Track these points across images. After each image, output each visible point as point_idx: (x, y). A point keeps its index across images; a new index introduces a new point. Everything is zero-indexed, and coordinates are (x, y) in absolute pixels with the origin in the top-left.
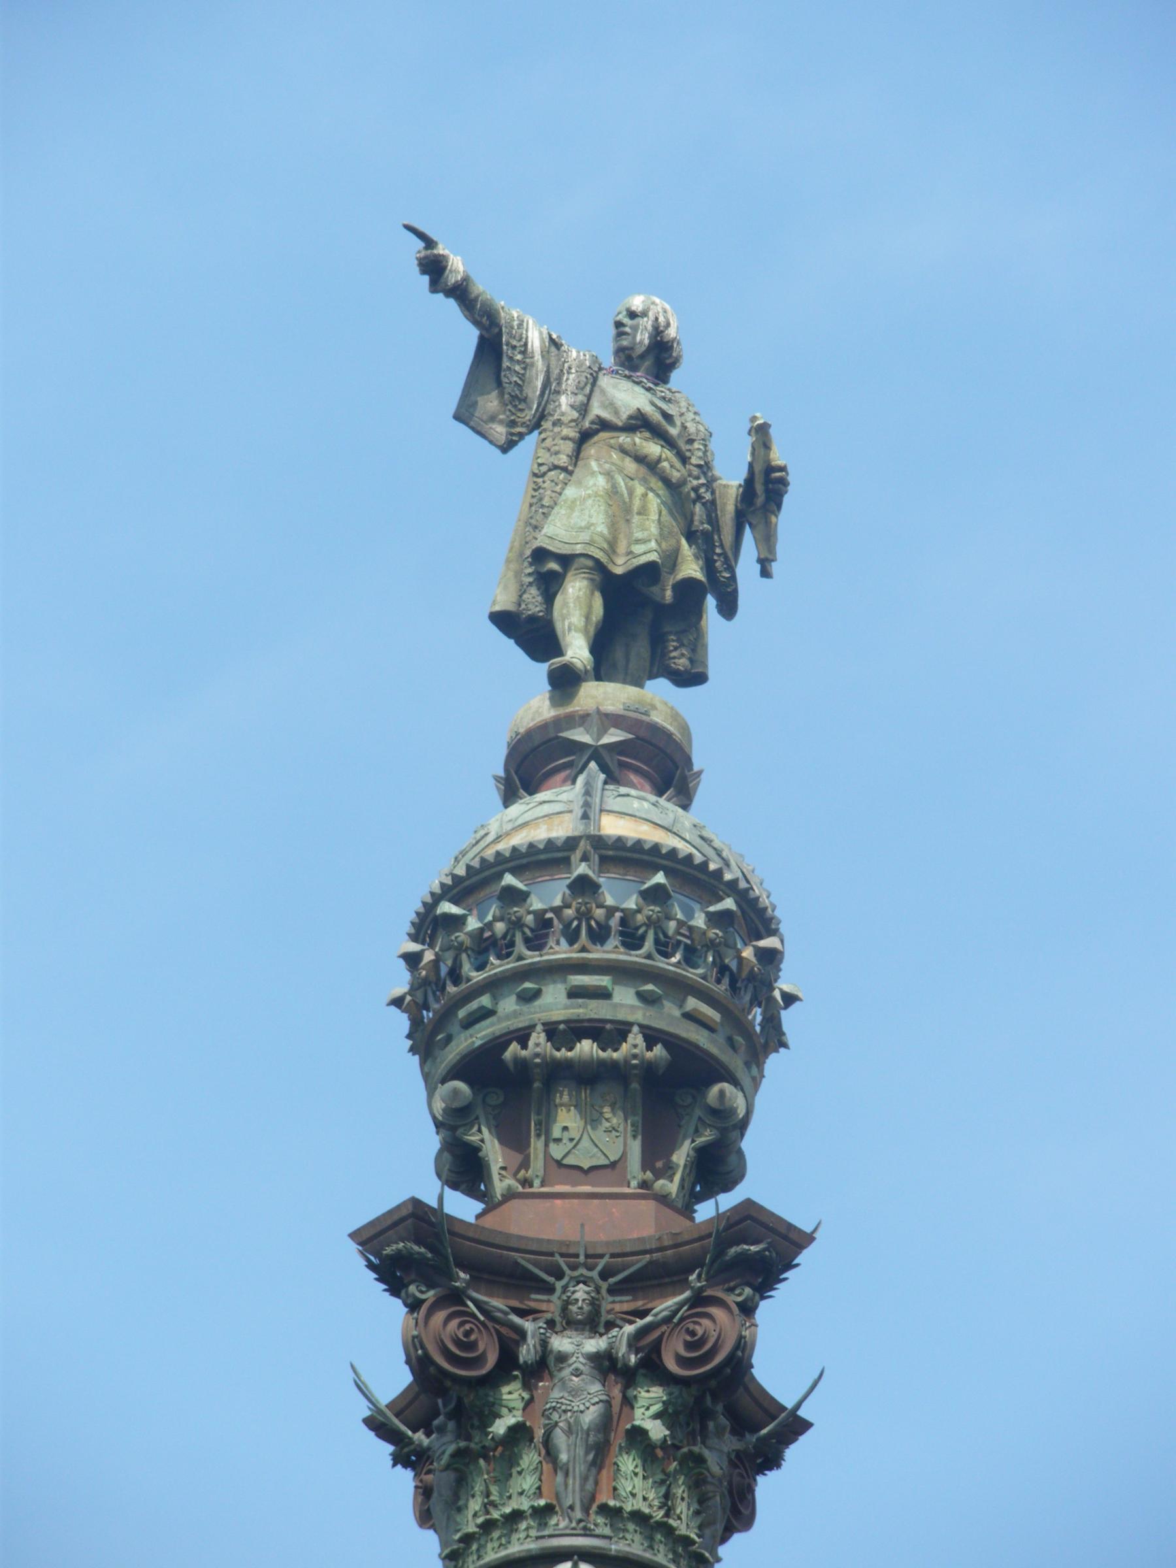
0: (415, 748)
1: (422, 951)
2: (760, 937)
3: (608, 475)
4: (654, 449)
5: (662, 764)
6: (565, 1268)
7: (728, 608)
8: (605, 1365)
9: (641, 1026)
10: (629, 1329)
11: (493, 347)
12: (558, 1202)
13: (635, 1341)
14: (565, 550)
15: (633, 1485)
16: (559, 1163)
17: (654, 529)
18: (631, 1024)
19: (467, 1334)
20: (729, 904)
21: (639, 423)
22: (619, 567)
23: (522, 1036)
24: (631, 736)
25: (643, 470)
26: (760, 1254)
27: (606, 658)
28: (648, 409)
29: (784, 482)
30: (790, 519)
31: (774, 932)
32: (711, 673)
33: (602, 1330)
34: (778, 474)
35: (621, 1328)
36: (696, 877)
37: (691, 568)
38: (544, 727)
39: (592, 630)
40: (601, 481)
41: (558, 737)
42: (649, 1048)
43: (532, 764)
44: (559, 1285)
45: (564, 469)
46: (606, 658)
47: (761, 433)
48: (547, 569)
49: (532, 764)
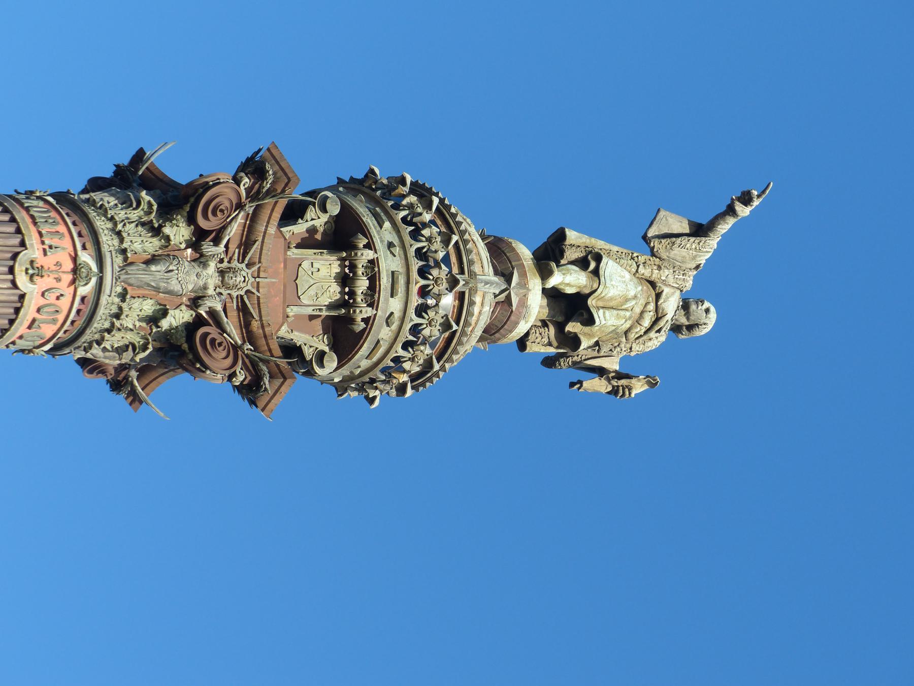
3: (635, 297)
4: (647, 323)
9: (375, 315)
12: (282, 265)
14: (601, 272)
16: (300, 265)
17: (610, 323)
18: (377, 310)
22: (591, 302)
23: (368, 246)
25: (636, 316)
39: (561, 287)
40: (632, 293)
41: (513, 268)
42: (363, 320)
44: (243, 266)
45: (637, 271)
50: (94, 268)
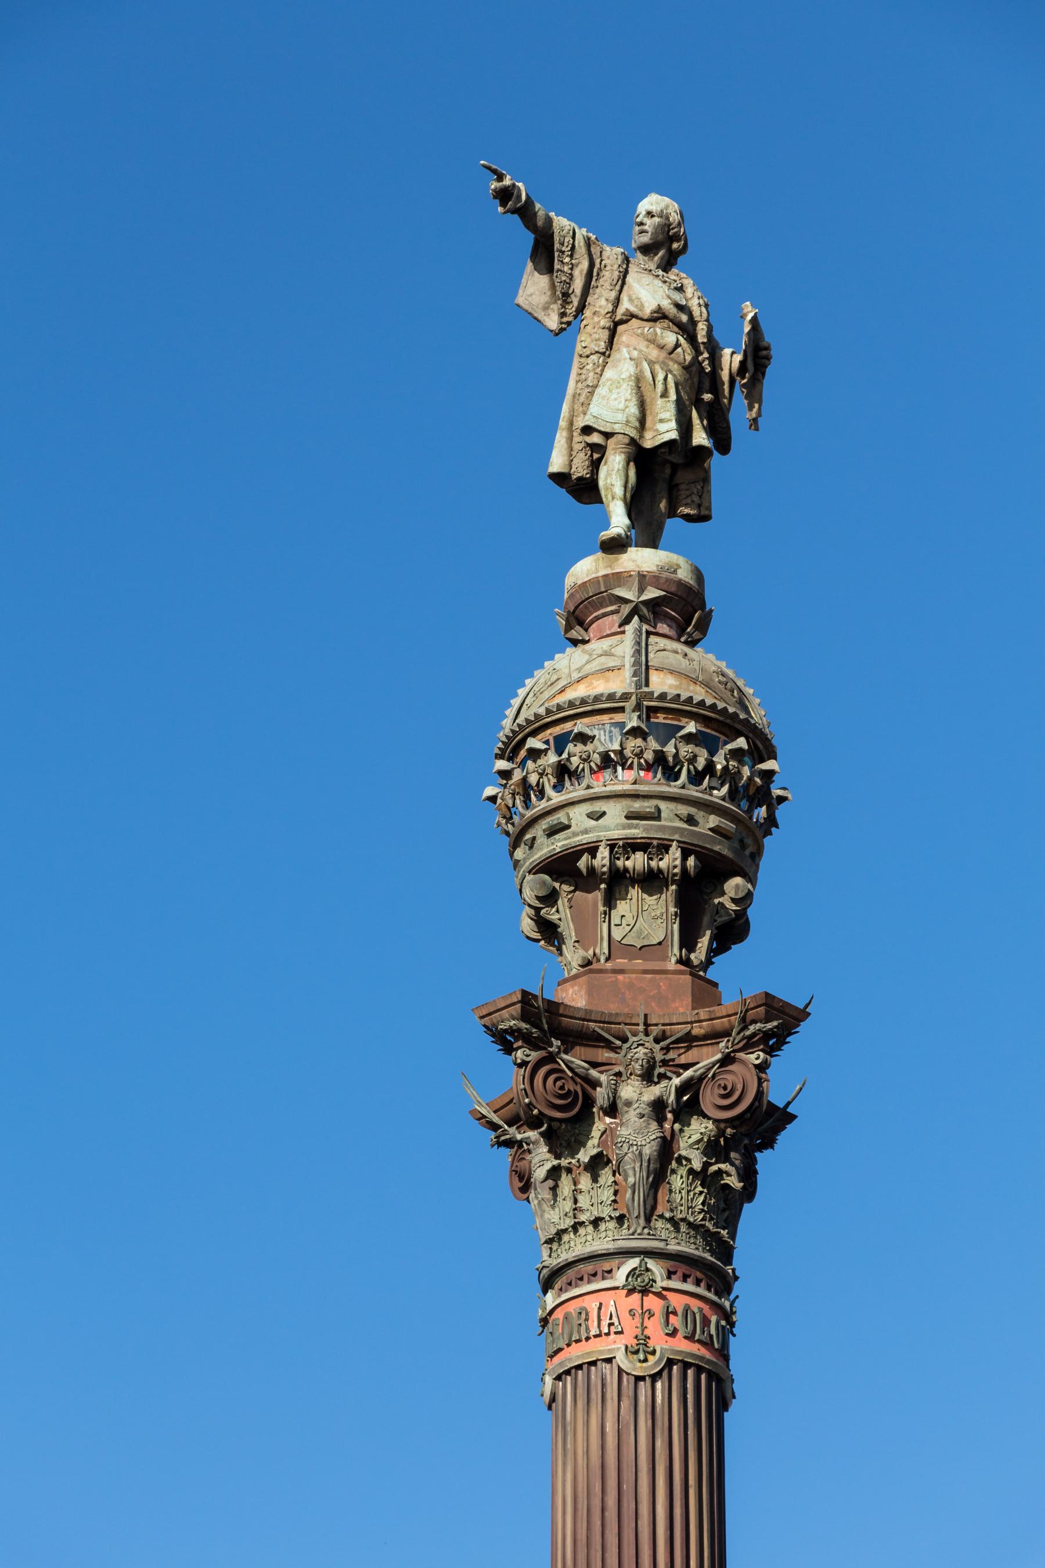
1: (513, 769)
2: (762, 761)
6: (629, 1035)
8: (658, 1107)
9: (678, 841)
10: (677, 1081)
12: (620, 977)
13: (681, 1091)
14: (608, 430)
18: (673, 841)
19: (562, 1088)
20: (741, 742)
24: (663, 593)
28: (666, 304)
29: (768, 358)
31: (773, 756)
32: (714, 513)
33: (656, 1080)
34: (765, 352)
35: (670, 1079)
38: (595, 581)
45: (603, 354)
50: (633, 1263)
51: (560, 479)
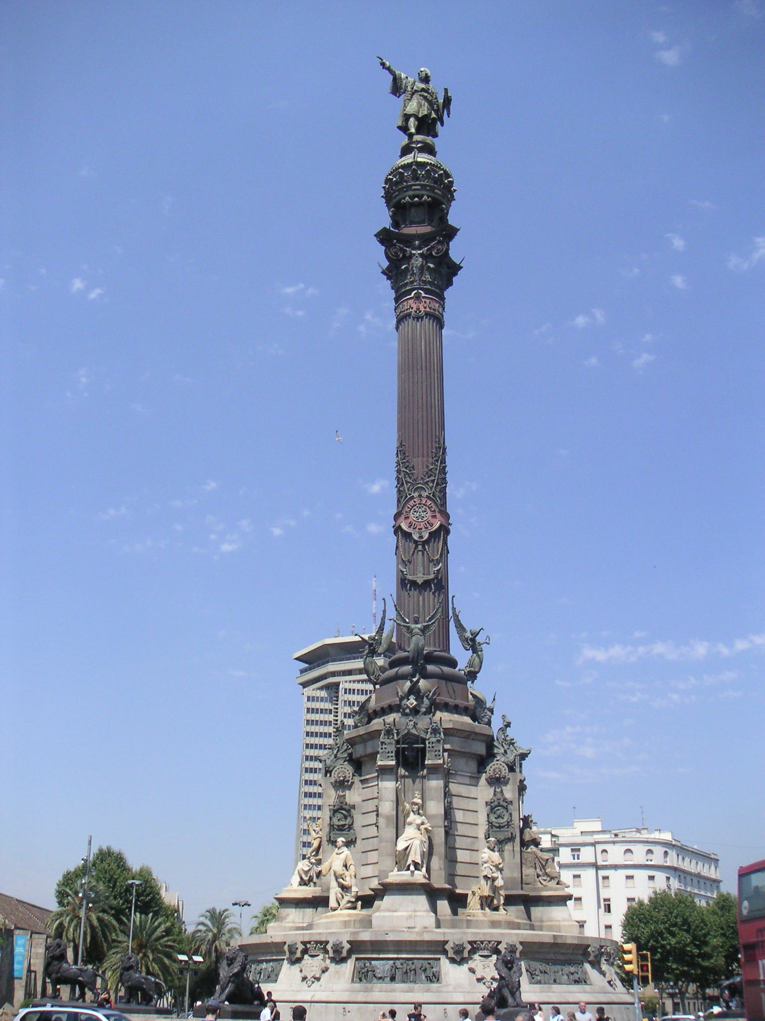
0: (386, 153)
5: (430, 150)
7: (442, 124)
8: (421, 255)
11: (396, 80)
15: (428, 277)
21: (423, 90)
26: (450, 233)
27: (419, 131)
30: (452, 106)
32: (439, 134)
36: (436, 167)
37: (434, 115)
43: (406, 151)
46: (419, 131)
47: (446, 90)
48: (407, 117)
49: (406, 151)
51: (399, 128)
